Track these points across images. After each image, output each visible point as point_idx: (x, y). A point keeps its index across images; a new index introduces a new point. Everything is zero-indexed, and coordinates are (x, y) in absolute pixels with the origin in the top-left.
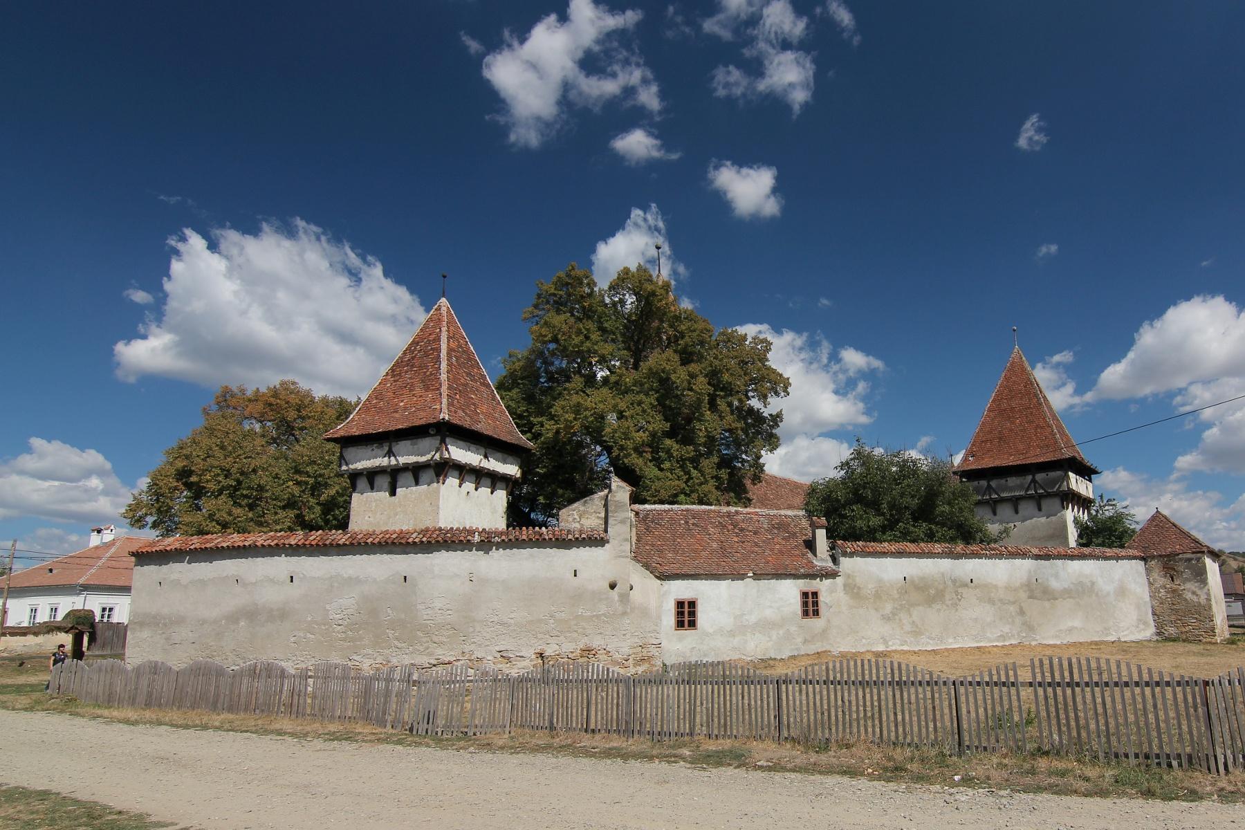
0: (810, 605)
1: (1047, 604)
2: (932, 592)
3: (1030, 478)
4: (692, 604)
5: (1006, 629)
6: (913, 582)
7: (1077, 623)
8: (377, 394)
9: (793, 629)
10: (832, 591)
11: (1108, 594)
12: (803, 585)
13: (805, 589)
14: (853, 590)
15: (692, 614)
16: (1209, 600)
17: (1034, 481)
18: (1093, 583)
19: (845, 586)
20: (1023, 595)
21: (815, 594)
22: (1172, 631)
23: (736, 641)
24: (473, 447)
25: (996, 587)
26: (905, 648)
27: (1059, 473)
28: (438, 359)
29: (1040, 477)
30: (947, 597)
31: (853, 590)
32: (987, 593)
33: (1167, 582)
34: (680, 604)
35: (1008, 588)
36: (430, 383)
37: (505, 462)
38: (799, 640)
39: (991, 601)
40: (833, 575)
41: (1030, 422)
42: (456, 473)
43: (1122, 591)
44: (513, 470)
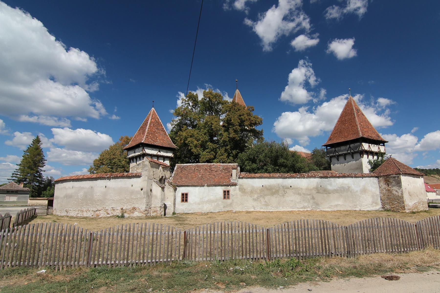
0: (226, 194)
1: (325, 195)
2: (274, 191)
3: (348, 146)
4: (187, 194)
5: (306, 204)
6: (266, 187)
9: (220, 203)
10: (234, 190)
11: (357, 191)
12: (224, 188)
13: (225, 190)
14: (242, 190)
15: (187, 197)
16: (402, 194)
17: (350, 147)
19: (239, 189)
20: (314, 192)
21: (228, 192)
22: (388, 207)
23: (200, 206)
24: (154, 149)
25: (302, 189)
26: (262, 210)
27: (358, 144)
29: (352, 145)
30: (280, 192)
31: (242, 190)
32: (297, 191)
34: (183, 194)
35: (307, 189)
37: (167, 152)
38: (222, 206)
39: (299, 194)
40: (235, 185)
42: (150, 157)
43: (364, 190)
44: (170, 155)
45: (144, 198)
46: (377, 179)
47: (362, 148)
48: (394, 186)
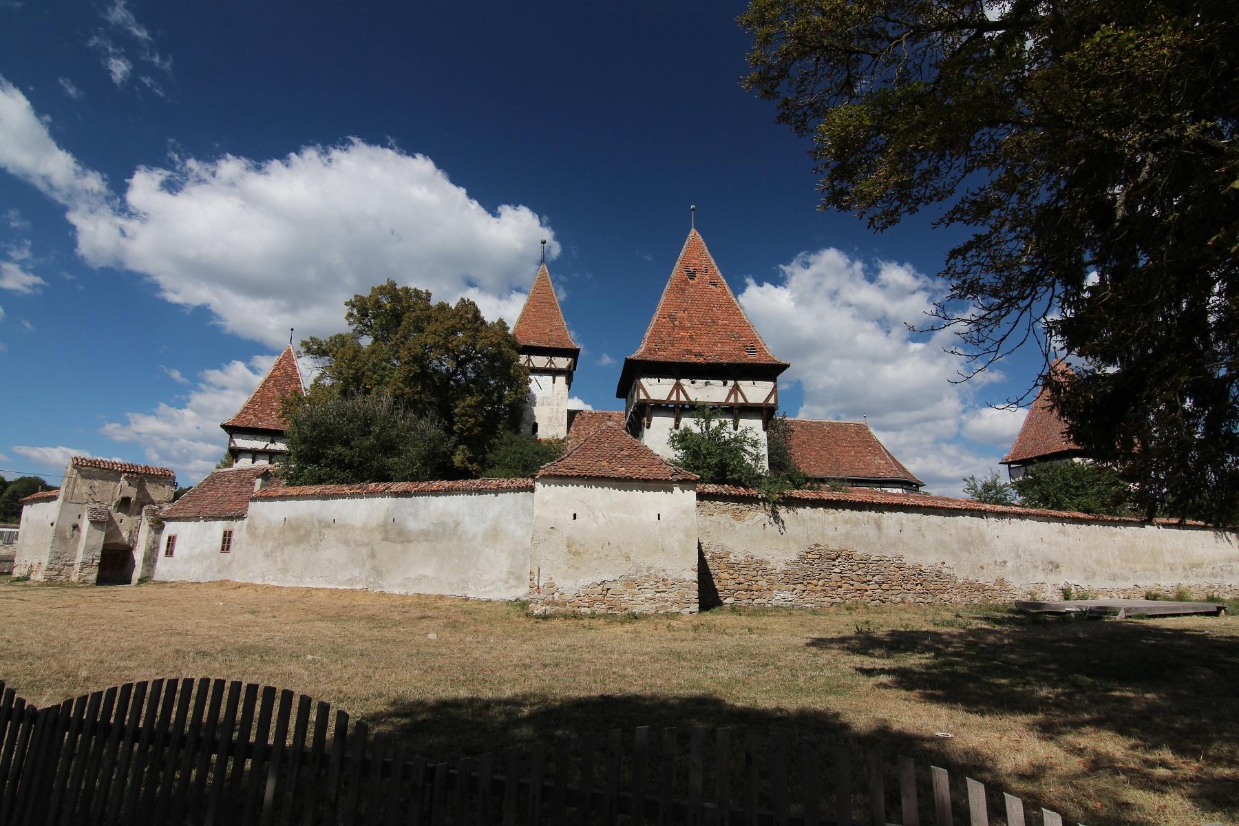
1: (399, 547)
5: (356, 573)
7: (429, 572)
11: (475, 537)
18: (457, 524)
19: (249, 526)
20: (378, 536)
25: (353, 527)
38: (216, 569)
39: (347, 543)
43: (494, 535)
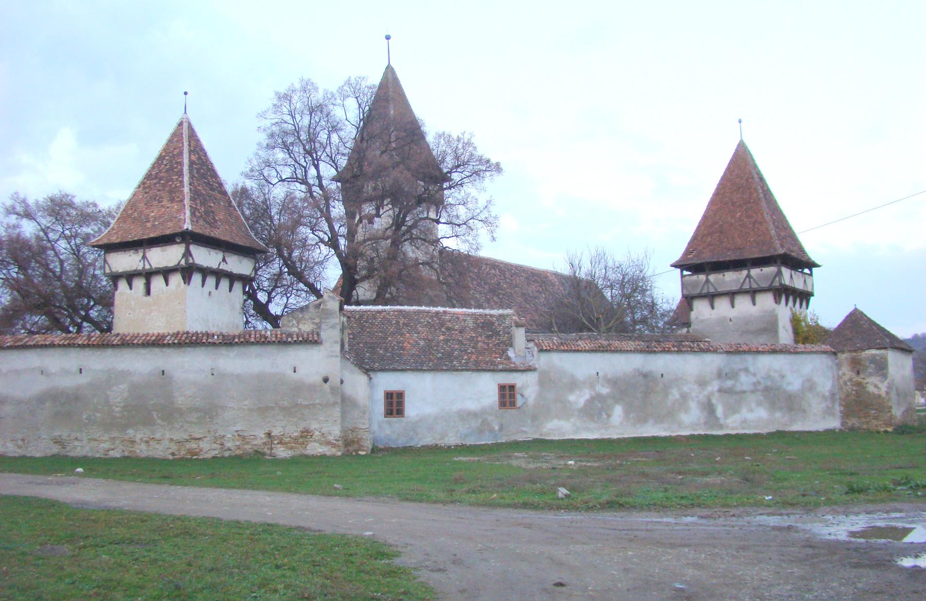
3: (745, 273)
4: (400, 395)
8: (132, 204)
17: (748, 276)
28: (181, 173)
29: (755, 272)
33: (854, 375)
34: (389, 395)
36: (174, 194)
41: (749, 217)
45: (335, 404)
46: (833, 357)
47: (780, 279)
48: (871, 375)
